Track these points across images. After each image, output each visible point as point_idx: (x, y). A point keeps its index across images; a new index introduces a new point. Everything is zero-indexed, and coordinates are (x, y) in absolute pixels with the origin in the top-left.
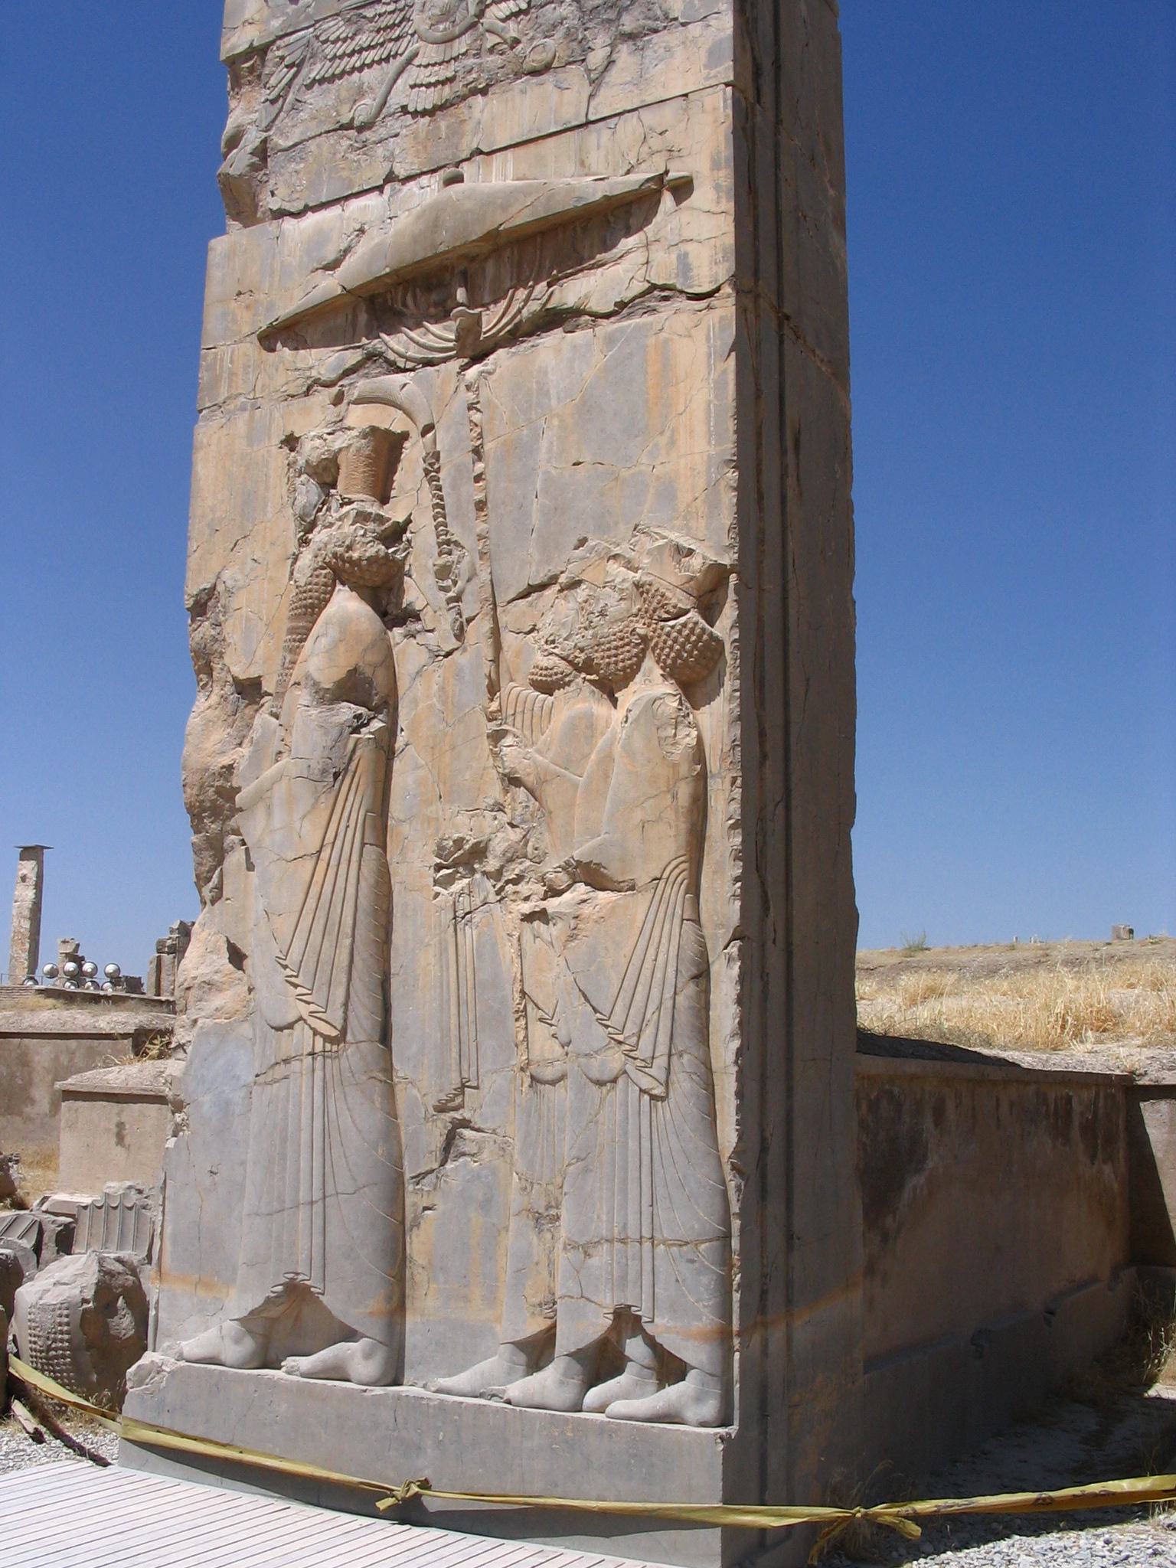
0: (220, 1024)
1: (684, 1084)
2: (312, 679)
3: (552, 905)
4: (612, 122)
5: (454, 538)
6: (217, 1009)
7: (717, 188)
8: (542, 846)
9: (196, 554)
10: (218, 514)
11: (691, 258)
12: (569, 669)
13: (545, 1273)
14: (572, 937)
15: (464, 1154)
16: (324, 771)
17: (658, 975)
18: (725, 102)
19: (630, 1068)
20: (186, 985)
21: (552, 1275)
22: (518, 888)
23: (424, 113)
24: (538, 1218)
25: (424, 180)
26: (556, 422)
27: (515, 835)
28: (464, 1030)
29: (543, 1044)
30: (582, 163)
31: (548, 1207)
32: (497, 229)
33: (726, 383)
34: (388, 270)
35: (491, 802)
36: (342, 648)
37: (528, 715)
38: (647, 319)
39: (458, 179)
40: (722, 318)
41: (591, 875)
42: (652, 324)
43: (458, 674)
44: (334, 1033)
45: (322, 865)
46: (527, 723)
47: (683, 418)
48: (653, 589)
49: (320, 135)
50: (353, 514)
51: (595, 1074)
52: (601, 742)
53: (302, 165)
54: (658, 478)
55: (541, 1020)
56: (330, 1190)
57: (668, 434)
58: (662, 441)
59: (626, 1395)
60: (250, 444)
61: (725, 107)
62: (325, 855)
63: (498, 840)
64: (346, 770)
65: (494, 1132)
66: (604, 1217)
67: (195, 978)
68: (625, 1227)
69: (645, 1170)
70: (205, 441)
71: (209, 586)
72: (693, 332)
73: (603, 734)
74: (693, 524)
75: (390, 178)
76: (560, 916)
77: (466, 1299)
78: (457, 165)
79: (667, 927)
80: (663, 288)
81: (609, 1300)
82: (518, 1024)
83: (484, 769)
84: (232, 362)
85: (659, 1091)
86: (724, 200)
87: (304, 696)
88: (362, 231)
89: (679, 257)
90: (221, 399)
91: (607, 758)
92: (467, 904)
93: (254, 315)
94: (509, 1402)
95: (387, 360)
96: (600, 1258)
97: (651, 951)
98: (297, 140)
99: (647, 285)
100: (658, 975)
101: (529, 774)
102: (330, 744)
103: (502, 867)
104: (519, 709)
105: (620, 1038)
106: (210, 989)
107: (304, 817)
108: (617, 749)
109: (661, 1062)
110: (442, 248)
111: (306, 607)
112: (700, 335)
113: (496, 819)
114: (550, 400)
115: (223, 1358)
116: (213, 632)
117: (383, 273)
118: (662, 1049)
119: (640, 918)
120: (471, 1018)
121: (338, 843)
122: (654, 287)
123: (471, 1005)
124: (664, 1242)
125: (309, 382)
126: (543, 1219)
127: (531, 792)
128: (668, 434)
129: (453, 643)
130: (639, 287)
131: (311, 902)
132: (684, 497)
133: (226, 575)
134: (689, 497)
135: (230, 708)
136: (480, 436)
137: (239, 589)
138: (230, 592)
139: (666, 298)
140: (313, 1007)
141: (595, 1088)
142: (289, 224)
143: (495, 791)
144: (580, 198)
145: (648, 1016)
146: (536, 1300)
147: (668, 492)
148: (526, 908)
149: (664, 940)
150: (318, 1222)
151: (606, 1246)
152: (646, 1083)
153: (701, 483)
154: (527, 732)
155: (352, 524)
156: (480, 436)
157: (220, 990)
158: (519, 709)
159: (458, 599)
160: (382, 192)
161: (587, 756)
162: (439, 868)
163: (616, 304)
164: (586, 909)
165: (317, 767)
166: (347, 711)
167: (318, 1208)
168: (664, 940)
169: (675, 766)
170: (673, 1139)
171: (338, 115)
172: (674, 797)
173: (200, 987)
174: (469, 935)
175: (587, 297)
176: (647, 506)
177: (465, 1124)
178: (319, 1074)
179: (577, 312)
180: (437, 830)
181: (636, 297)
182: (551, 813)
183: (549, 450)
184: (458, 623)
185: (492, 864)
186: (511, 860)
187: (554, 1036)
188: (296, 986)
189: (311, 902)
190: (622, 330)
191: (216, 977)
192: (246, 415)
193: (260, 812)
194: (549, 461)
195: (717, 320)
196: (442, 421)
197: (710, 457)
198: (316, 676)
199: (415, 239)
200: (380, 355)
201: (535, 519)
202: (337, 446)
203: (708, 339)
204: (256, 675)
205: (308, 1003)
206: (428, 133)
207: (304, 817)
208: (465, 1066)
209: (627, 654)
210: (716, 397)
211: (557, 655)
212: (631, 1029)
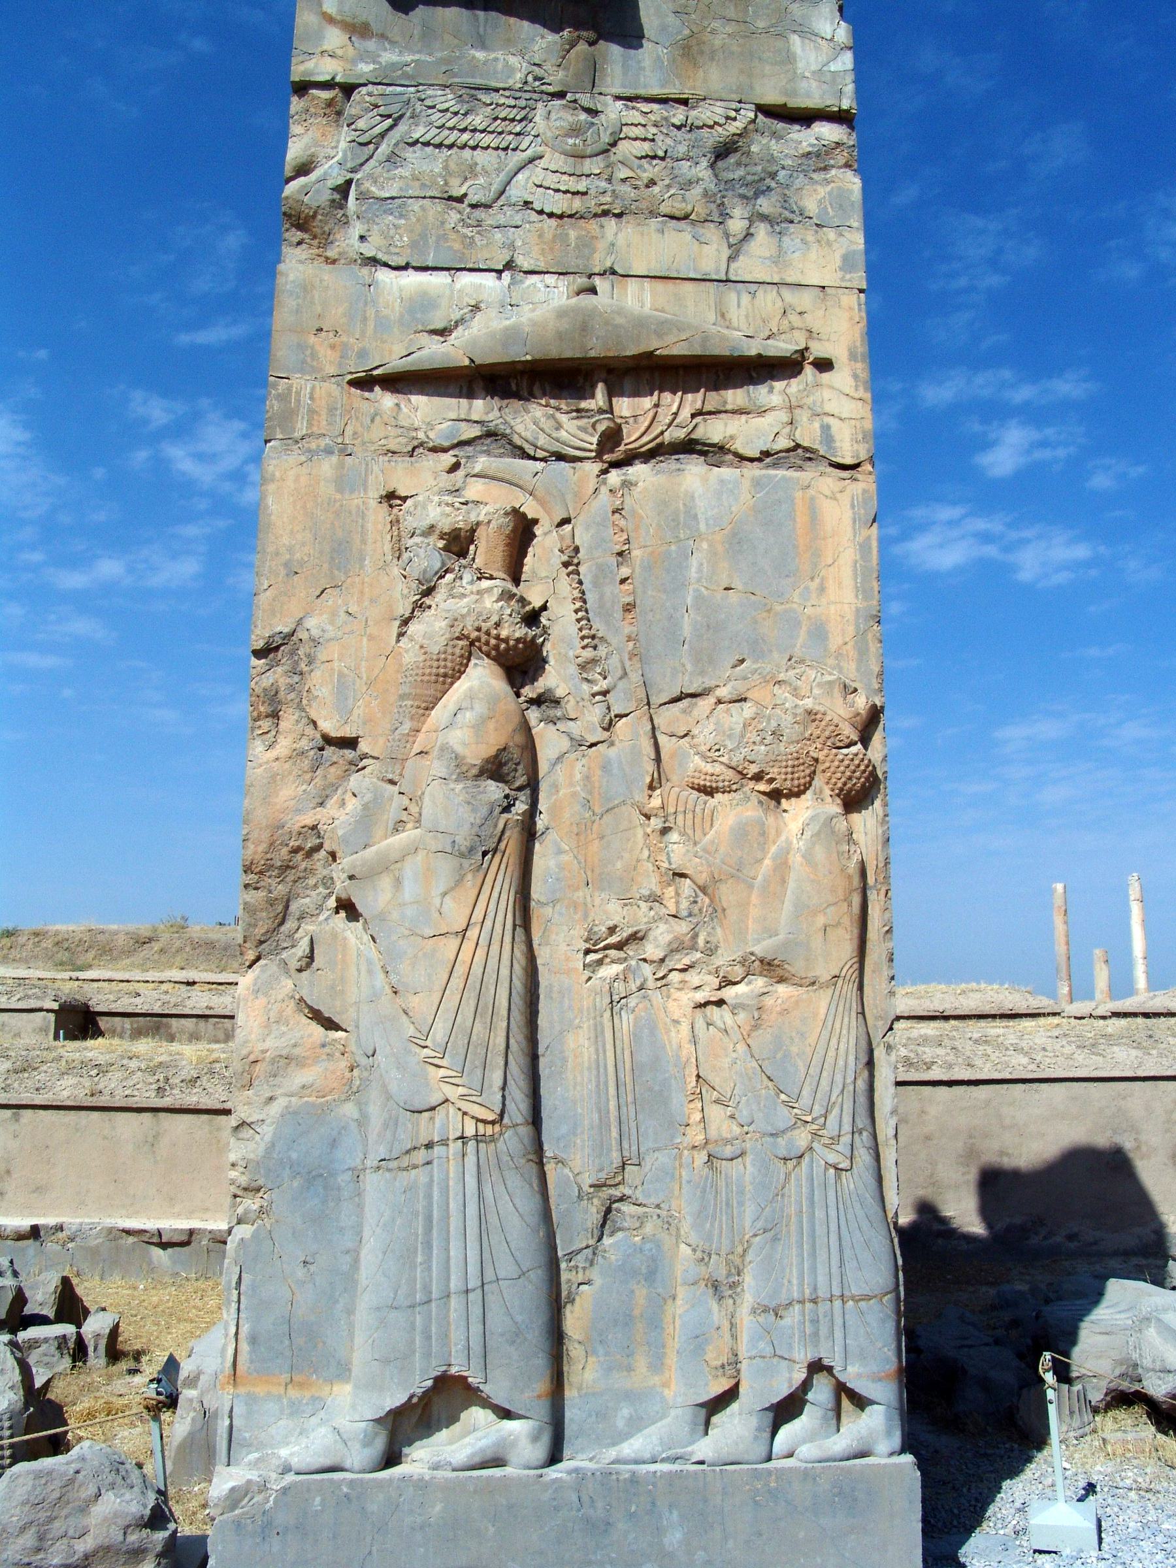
0: (313, 1105)
1: (864, 1157)
2: (453, 752)
3: (729, 993)
4: (753, 287)
5: (600, 634)
6: (303, 1087)
7: (855, 376)
8: (713, 939)
9: (268, 593)
10: (298, 556)
11: (834, 430)
12: (737, 777)
13: (727, 1336)
14: (756, 1027)
15: (620, 1229)
16: (471, 850)
17: (841, 1063)
18: (860, 305)
19: (815, 1145)
20: (252, 1058)
21: (734, 1337)
22: (687, 976)
23: (551, 215)
25: (550, 279)
26: (705, 545)
27: (683, 928)
28: (624, 1110)
29: (720, 1123)
30: (723, 315)
32: (652, 352)
33: (870, 548)
34: (529, 358)
35: (647, 893)
36: (491, 725)
37: (690, 816)
38: (791, 473)
39: (593, 291)
40: (864, 491)
41: (771, 968)
42: (798, 479)
43: (606, 767)
44: (491, 1117)
45: (468, 946)
46: (689, 823)
47: (831, 569)
48: (828, 718)
49: (424, 198)
50: (497, 592)
53: (403, 221)
54: (809, 618)
55: (717, 1102)
56: (489, 1275)
57: (817, 581)
58: (814, 585)
59: (811, 1437)
60: (340, 489)
61: (860, 310)
62: (473, 933)
63: (659, 931)
64: (495, 850)
65: (658, 1206)
66: (795, 1281)
67: (264, 1052)
68: (815, 1289)
69: (834, 1238)
70: (277, 474)
71: (286, 630)
72: (838, 495)
73: (774, 843)
74: (844, 664)
75: (509, 265)
76: (743, 1006)
77: (630, 1369)
78: (590, 276)
79: (846, 1020)
80: (806, 449)
81: (804, 1355)
82: (692, 1105)
83: (638, 861)
84: (311, 398)
85: (845, 1164)
86: (861, 389)
87: (437, 767)
88: (476, 308)
89: (822, 427)
90: (297, 435)
91: (782, 866)
92: (622, 989)
93: (341, 357)
94: (702, 1463)
95: (510, 443)
96: (793, 1317)
97: (834, 1041)
98: (395, 195)
99: (793, 444)
100: (841, 1063)
102: (478, 821)
103: (666, 956)
104: (681, 809)
105: (809, 1119)
107: (444, 894)
108: (796, 859)
109: (846, 1139)
110: (592, 354)
112: (845, 499)
113: (651, 909)
114: (698, 523)
115: (347, 1465)
116: (288, 680)
117: (523, 359)
118: (847, 1128)
119: (823, 1011)
120: (630, 1099)
121: (488, 923)
122: (798, 446)
123: (629, 1087)
124: (853, 1298)
125: (416, 443)
128: (817, 581)
129: (600, 735)
130: (783, 443)
131: (457, 982)
132: (835, 641)
133: (311, 623)
134: (840, 641)
135: (306, 764)
136: (628, 541)
137: (328, 640)
138: (316, 643)
139: (810, 459)
140: (461, 1091)
142: (383, 275)
143: (650, 883)
144: (734, 348)
145: (833, 1099)
147: (819, 632)
148: (701, 997)
149: (844, 1032)
150: (476, 1311)
151: (797, 1307)
152: (832, 1158)
153: (851, 630)
154: (690, 832)
155: (497, 601)
156: (628, 541)
157: (303, 1066)
158: (681, 809)
159: (605, 693)
160: (500, 278)
161: (760, 861)
162: (587, 952)
163: (762, 452)
164: (768, 1001)
165: (463, 842)
166: (494, 790)
167: (475, 1297)
168: (844, 1032)
169: (850, 877)
170: (857, 1206)
171: (446, 184)
172: (850, 905)
173: (273, 1061)
174: (626, 1021)
175: (732, 437)
176: (800, 641)
178: (471, 1159)
179: (721, 449)
180: (586, 916)
181: (781, 451)
182: (724, 910)
183: (700, 570)
184: (608, 718)
185: (652, 950)
186: (677, 950)
187: (732, 1117)
189: (457, 982)
190: (770, 477)
191: (296, 1051)
192: (334, 459)
193: (386, 882)
194: (699, 580)
195: (860, 492)
196: (580, 518)
197: (858, 610)
198: (459, 749)
199: (560, 336)
200: (504, 436)
201: (687, 631)
202: (473, 518)
203: (853, 506)
204: (354, 735)
206: (554, 236)
207: (444, 894)
208: (626, 1145)
209: (802, 773)
210: (862, 557)
211: (722, 763)
212: (818, 1110)
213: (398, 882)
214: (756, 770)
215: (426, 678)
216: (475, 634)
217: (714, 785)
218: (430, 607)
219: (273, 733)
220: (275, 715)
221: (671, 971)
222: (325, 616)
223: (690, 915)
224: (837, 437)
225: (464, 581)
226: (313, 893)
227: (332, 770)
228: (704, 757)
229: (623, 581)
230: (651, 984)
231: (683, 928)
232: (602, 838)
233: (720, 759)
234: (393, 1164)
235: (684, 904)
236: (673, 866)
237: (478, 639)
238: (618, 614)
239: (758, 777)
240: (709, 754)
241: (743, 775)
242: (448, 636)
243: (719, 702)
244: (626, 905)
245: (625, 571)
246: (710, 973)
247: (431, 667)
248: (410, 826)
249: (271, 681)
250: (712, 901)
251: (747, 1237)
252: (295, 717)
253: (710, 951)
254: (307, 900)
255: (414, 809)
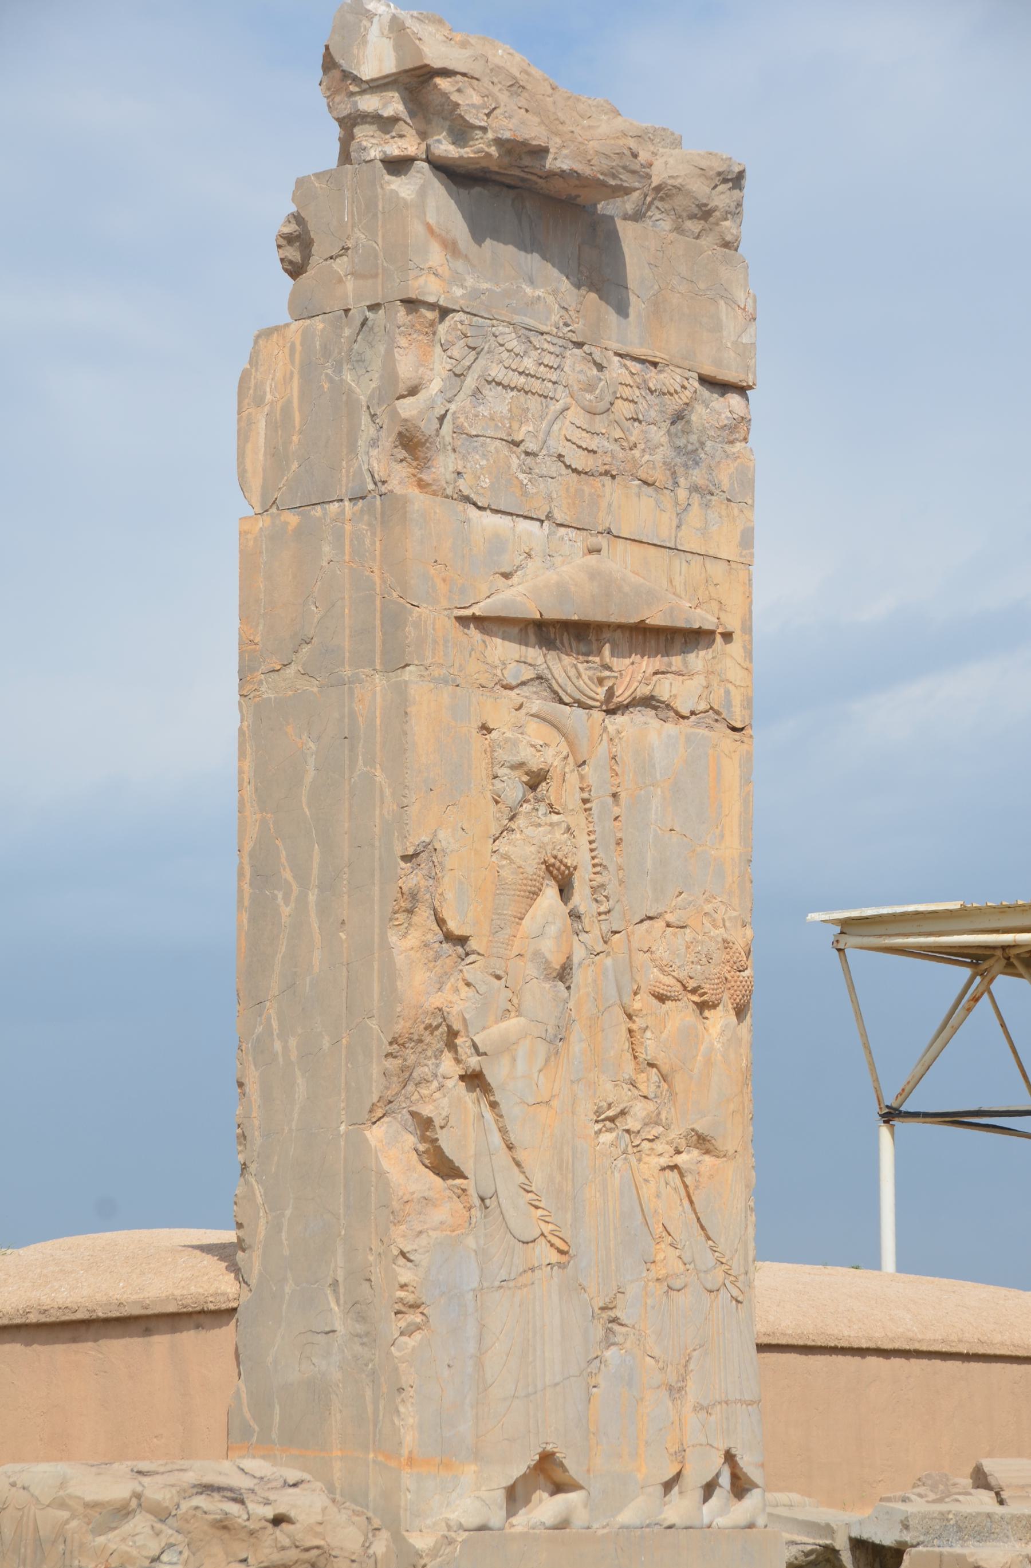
2: (544, 957)
15: (613, 1344)
20: (405, 1199)
24: (671, 1388)
31: (678, 1381)
32: (643, 621)
41: (702, 1142)
51: (709, 1287)
52: (703, 1048)
57: (720, 828)
65: (633, 1327)
67: (413, 1193)
71: (427, 840)
91: (708, 1062)
95: (550, 687)
101: (665, 1064)
106: (427, 1204)
107: (540, 1071)
111: (530, 892)
117: (573, 618)
122: (712, 708)
126: (675, 1391)
127: (664, 1078)
130: (703, 706)
133: (441, 835)
141: (707, 1294)
146: (672, 1451)
148: (664, 1161)
151: (719, 1407)
152: (735, 1292)
157: (435, 1206)
175: (675, 696)
177: (614, 1320)
188: (537, 1207)
193: (505, 1060)
198: (548, 955)
200: (547, 680)
201: (649, 864)
203: (740, 767)
205: (548, 1223)
207: (540, 1071)
211: (674, 977)
213: (514, 1060)
214: (695, 985)
215: (522, 893)
216: (552, 860)
217: (669, 994)
218: (513, 831)
219: (406, 925)
220: (410, 911)
221: (643, 1140)
222: (449, 830)
223: (655, 1097)
224: (734, 703)
225: (540, 813)
226: (430, 1063)
227: (447, 961)
228: (662, 971)
229: (616, 819)
230: (630, 1150)
231: (651, 1106)
232: (603, 1031)
233: (673, 973)
234: (512, 1284)
235: (653, 1088)
236: (649, 1058)
237: (553, 865)
238: (613, 846)
239: (694, 991)
240: (666, 969)
241: (685, 988)
242: (537, 860)
243: (668, 925)
244: (616, 1085)
245: (616, 811)
246: (667, 1143)
247: (526, 885)
248: (513, 1014)
249: (415, 882)
250: (669, 1087)
251: (689, 1351)
252: (426, 914)
253: (667, 1128)
254: (426, 1069)
255: (515, 1001)
